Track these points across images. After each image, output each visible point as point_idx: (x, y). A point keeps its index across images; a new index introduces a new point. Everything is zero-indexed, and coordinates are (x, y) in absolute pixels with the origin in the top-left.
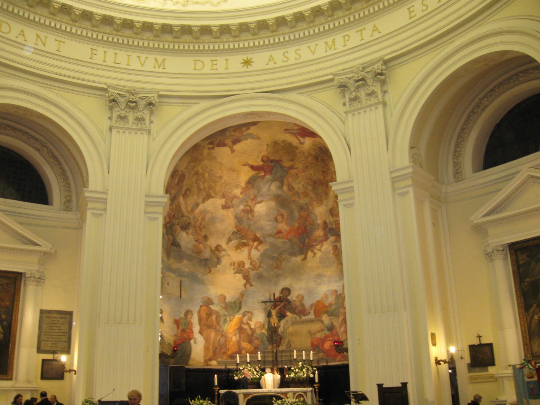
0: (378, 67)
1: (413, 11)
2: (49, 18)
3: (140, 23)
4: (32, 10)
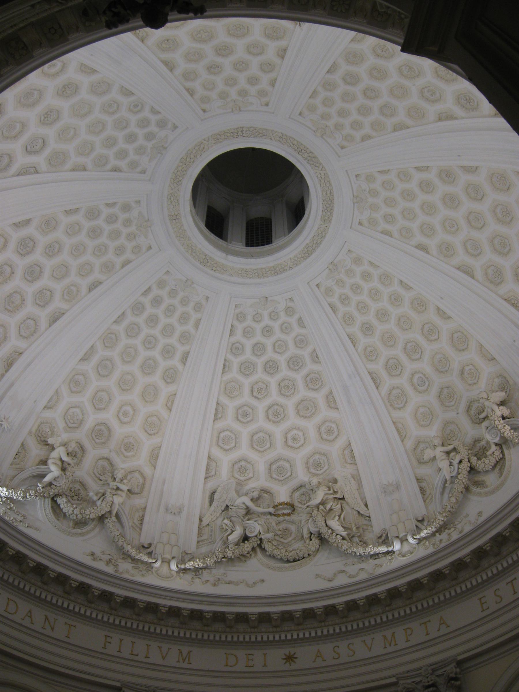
0: (451, 669)
1: (486, 602)
2: (62, 597)
3: (166, 607)
4: (46, 587)
